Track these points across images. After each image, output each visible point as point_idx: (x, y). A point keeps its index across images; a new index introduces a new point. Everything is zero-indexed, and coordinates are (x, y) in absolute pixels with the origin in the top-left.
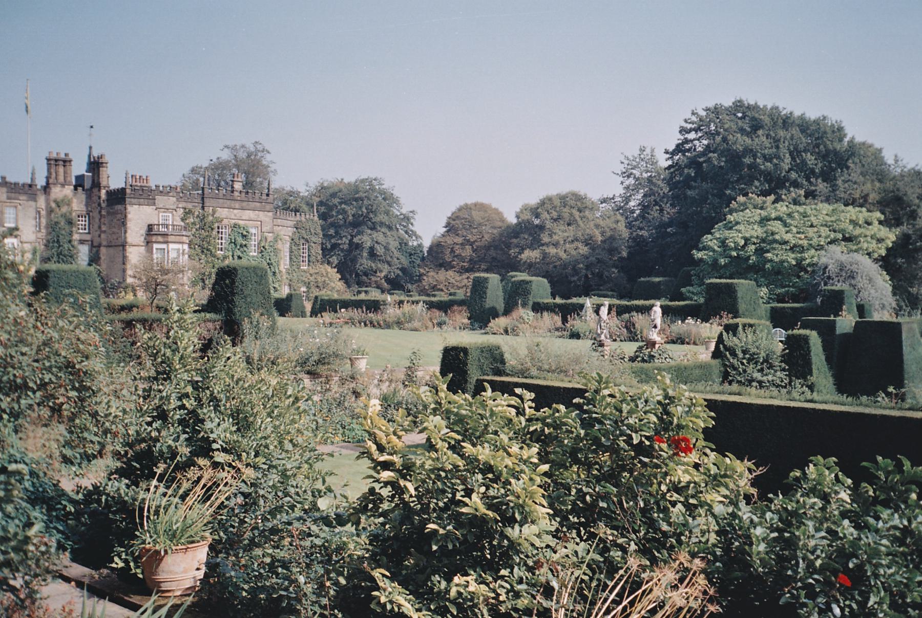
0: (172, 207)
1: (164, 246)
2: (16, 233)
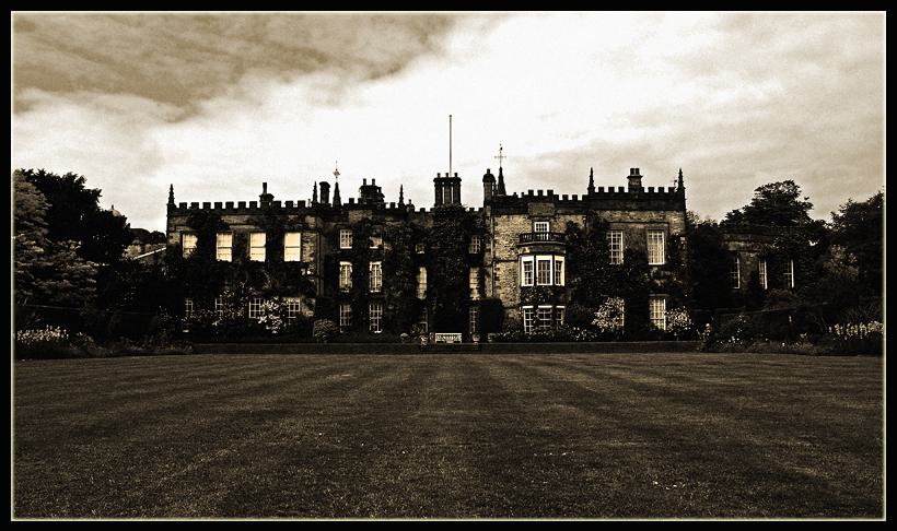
1: (531, 258)
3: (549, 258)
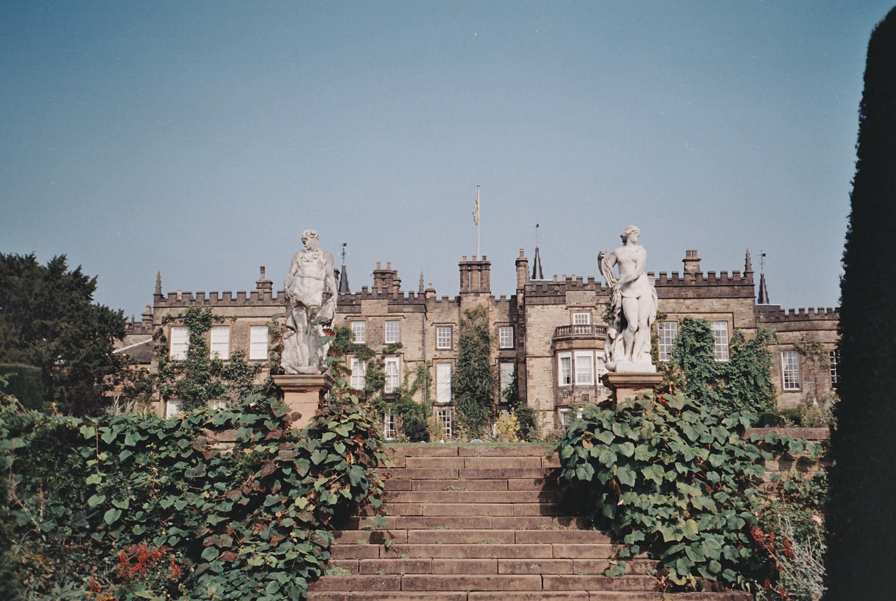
0: (590, 304)
1: (568, 354)
2: (398, 350)
3: (590, 353)
